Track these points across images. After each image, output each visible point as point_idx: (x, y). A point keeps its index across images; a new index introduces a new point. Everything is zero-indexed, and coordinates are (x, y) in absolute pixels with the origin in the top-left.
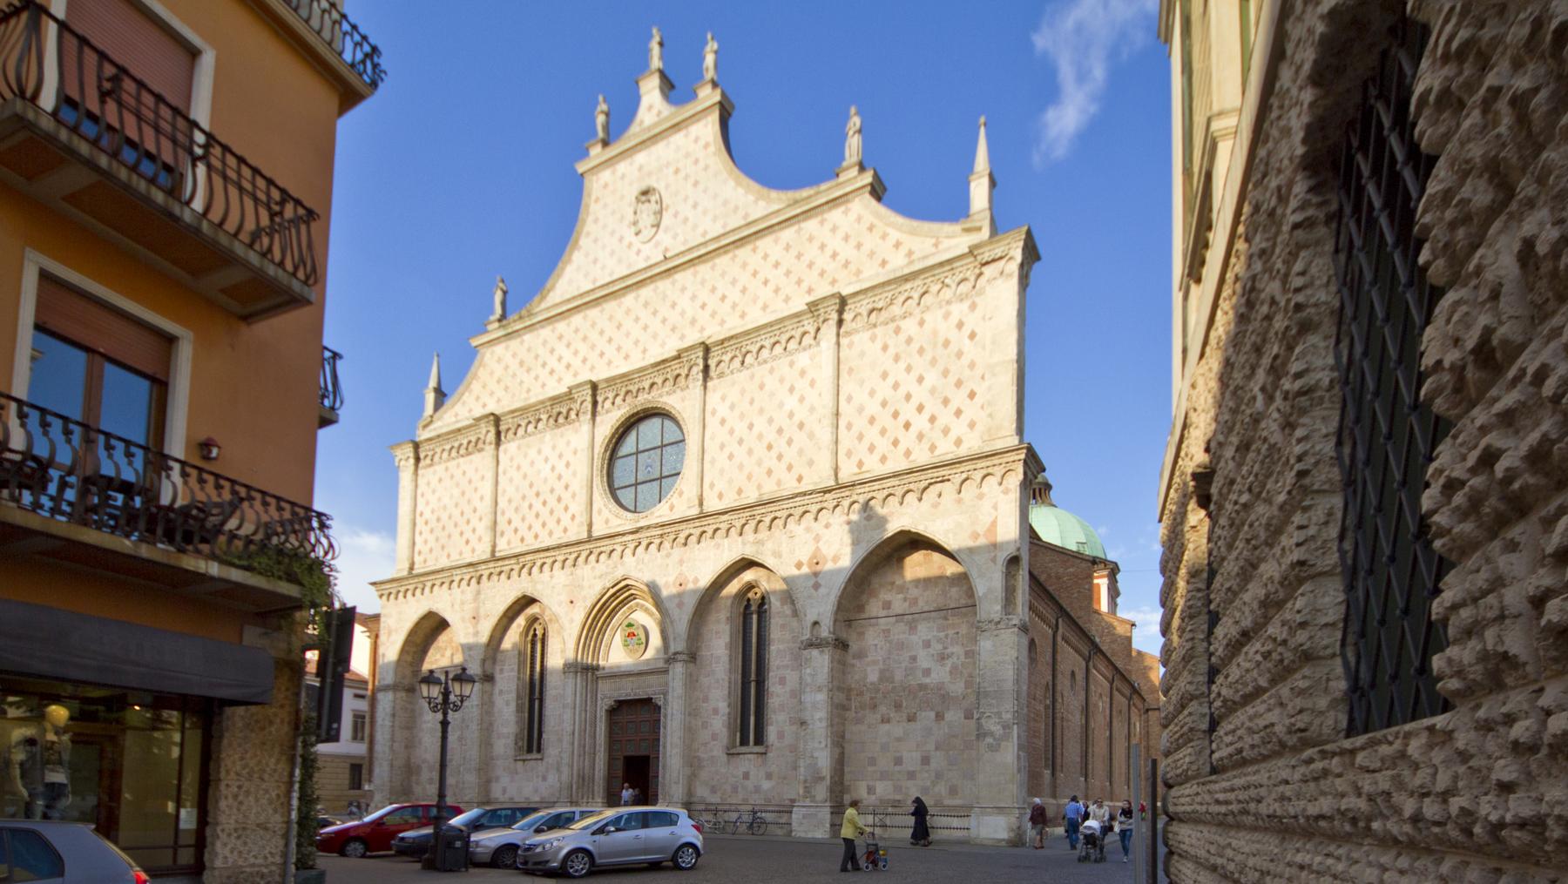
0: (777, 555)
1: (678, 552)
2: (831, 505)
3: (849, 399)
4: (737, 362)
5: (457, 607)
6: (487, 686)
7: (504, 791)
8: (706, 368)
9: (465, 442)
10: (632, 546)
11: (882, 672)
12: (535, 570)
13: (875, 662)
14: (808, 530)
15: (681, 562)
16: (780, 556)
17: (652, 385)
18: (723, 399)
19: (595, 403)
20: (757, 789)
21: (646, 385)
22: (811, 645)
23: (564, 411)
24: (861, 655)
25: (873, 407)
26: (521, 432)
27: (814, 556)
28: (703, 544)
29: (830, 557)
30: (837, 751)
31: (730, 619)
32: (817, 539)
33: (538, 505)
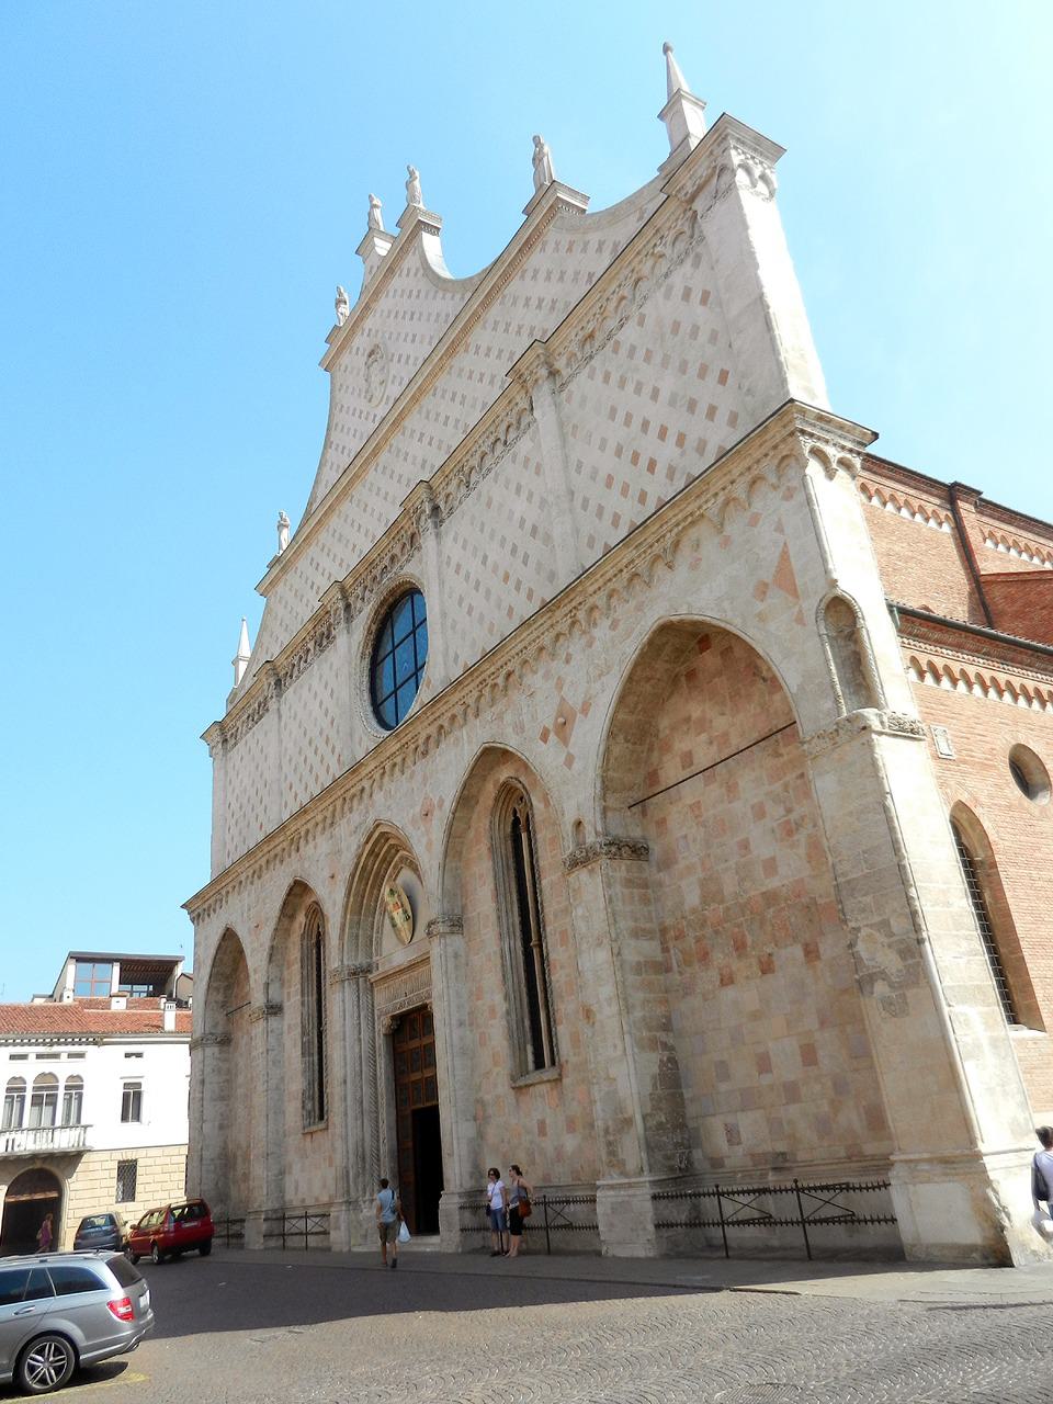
0: (520, 728)
2: (563, 627)
3: (580, 465)
4: (463, 490)
6: (274, 1022)
8: (436, 509)
9: (256, 705)
10: (377, 776)
11: (703, 883)
12: (302, 842)
13: (690, 869)
15: (425, 779)
17: (393, 559)
18: (455, 540)
19: (348, 606)
20: (559, 1154)
21: (386, 562)
22: (574, 864)
23: (324, 629)
24: (667, 863)
25: (607, 463)
26: (295, 673)
27: (560, 714)
28: (443, 746)
29: (579, 707)
30: (652, 1061)
31: (492, 850)
33: (309, 752)
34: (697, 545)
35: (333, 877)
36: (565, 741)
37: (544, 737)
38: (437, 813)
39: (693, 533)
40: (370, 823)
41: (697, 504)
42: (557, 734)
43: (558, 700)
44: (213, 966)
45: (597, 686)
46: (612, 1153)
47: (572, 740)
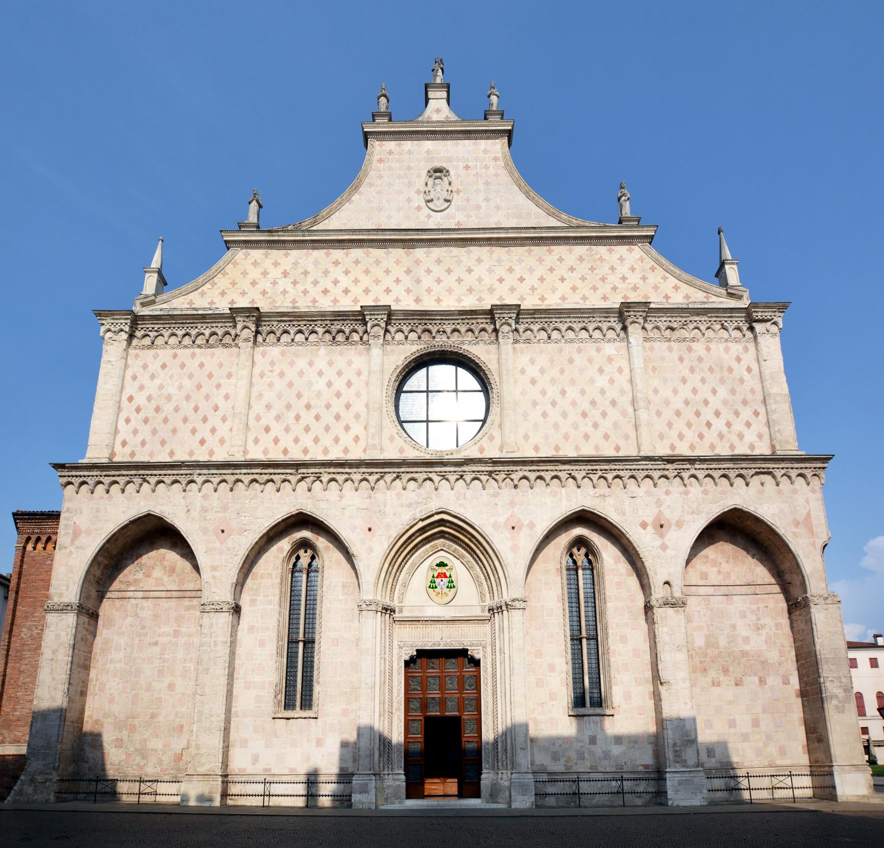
1: (507, 492)
5: (195, 513)
7: (255, 759)
14: (648, 493)
15: (512, 503)
16: (624, 514)
27: (657, 518)
32: (659, 503)
34: (762, 484)
35: (370, 530)
36: (662, 536)
37: (644, 525)
38: (525, 530)
39: (763, 477)
40: (433, 506)
41: (773, 466)
42: (654, 528)
43: (657, 510)
44: (108, 541)
45: (690, 517)
46: (679, 756)
47: (667, 537)
